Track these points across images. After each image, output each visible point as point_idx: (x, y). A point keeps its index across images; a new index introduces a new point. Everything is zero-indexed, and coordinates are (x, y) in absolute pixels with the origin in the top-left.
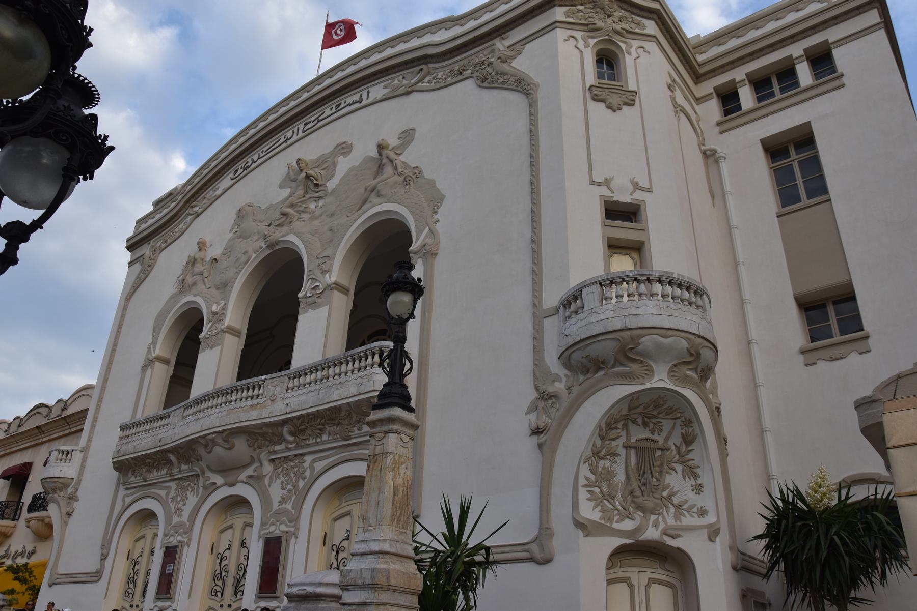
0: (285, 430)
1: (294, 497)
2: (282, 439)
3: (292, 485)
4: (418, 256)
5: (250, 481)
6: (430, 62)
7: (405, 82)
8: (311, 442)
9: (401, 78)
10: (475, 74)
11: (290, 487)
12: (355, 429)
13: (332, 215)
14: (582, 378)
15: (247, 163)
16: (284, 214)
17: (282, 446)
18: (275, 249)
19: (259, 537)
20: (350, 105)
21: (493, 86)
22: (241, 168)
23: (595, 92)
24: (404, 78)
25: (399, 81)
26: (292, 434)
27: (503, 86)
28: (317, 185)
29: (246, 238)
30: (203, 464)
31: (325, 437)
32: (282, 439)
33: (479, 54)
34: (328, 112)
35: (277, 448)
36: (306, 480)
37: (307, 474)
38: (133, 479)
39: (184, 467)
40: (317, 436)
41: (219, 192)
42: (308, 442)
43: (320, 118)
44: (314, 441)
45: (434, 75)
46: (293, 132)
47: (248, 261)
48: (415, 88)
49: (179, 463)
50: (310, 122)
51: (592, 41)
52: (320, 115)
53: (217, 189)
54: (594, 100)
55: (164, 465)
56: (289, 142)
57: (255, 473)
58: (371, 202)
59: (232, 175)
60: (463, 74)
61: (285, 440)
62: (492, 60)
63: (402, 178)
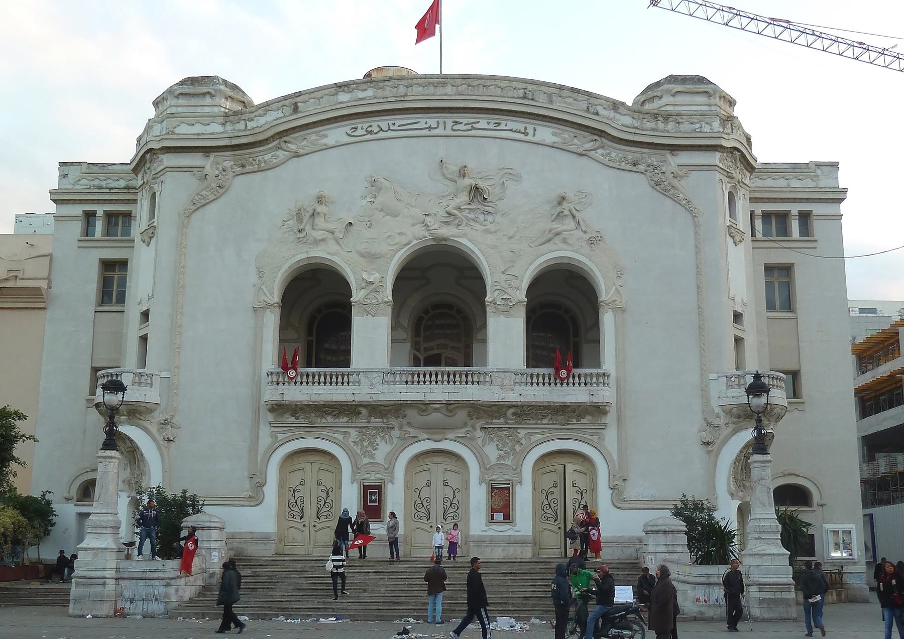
0: (511, 411)
1: (512, 457)
2: (504, 416)
3: (509, 449)
4: (609, 307)
5: (458, 439)
6: (604, 137)
7: (575, 139)
8: (531, 422)
9: (572, 135)
10: (648, 174)
11: (505, 449)
12: (574, 421)
13: (510, 238)
14: (734, 419)
15: (371, 126)
16: (449, 214)
17: (502, 420)
18: (441, 243)
19: (482, 481)
20: (511, 130)
21: (664, 193)
22: (362, 129)
23: (732, 231)
24: (576, 136)
25: (570, 136)
26: (514, 414)
27: (673, 197)
28: (485, 199)
29: (395, 216)
30: (404, 421)
31: (544, 421)
32: (504, 416)
33: (653, 158)
34: (483, 124)
35: (494, 421)
36: (522, 446)
37: (523, 441)
38: (292, 419)
39: (373, 419)
40: (538, 419)
41: (330, 141)
42: (528, 422)
43: (475, 126)
44: (534, 422)
45: (608, 151)
46: (438, 122)
47: (408, 244)
48: (588, 153)
49: (370, 415)
50: (461, 123)
51: (729, 185)
52: (474, 123)
53: (325, 136)
54: (730, 235)
55: (346, 414)
56: (433, 132)
57: (468, 435)
58: (555, 244)
59: (348, 129)
60: (636, 167)
61: (505, 417)
62: (664, 169)
63: (587, 237)
